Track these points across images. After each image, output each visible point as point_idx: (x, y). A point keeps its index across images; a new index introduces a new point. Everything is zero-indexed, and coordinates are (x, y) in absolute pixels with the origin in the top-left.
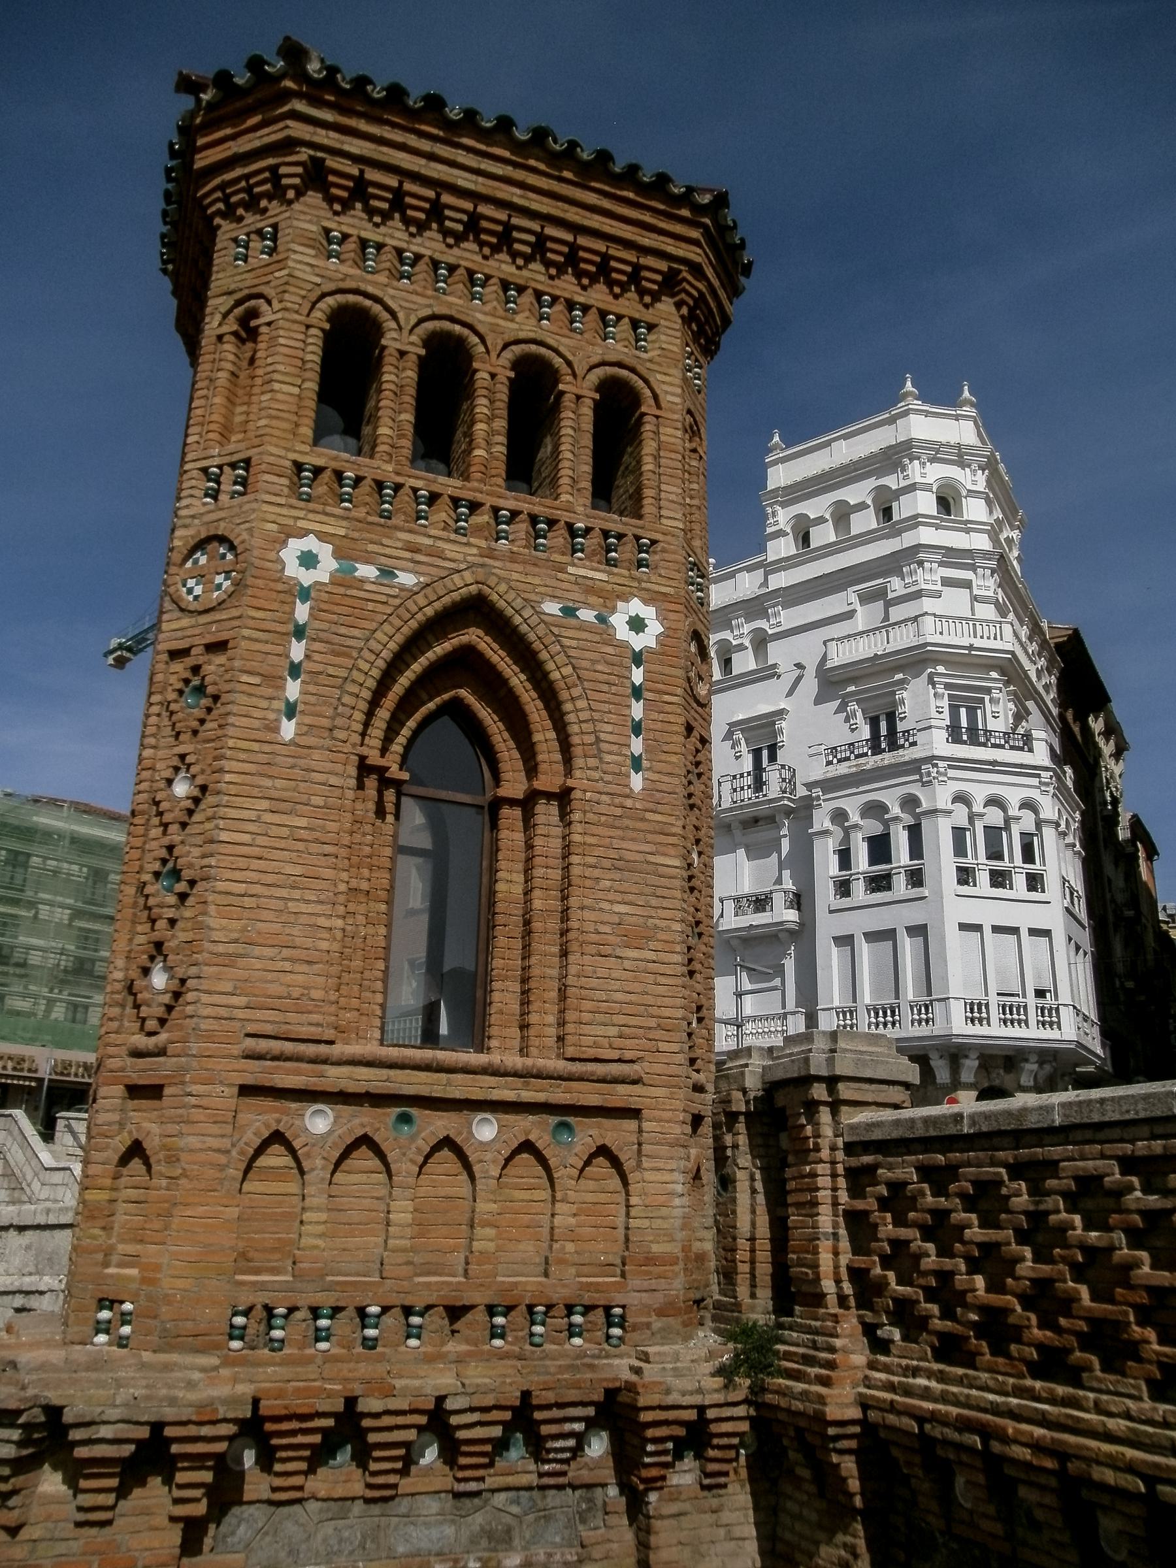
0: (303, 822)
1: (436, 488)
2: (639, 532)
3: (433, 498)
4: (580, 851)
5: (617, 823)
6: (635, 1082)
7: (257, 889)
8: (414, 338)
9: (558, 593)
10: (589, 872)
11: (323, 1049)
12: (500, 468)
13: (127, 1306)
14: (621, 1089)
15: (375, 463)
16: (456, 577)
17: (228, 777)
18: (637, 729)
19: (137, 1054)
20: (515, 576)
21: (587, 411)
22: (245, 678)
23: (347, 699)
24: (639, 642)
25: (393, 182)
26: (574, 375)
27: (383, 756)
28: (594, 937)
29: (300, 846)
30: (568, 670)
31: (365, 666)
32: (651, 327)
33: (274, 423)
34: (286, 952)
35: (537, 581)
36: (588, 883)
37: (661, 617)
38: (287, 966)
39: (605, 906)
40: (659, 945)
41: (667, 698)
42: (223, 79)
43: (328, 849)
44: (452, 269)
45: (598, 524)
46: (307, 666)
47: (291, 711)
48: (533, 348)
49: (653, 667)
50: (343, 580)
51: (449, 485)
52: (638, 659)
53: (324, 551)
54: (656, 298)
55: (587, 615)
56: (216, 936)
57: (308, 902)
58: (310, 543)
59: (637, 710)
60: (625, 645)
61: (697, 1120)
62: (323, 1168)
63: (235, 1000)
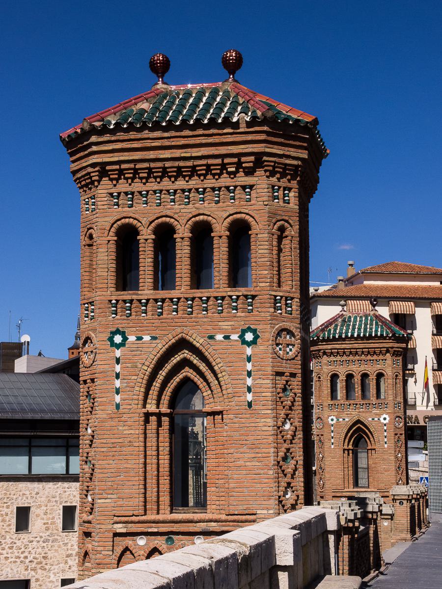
1: (350, 403)
3: (350, 405)
14: (385, 493)
18: (386, 437)
19: (320, 492)
23: (340, 441)
24: (385, 422)
25: (336, 351)
27: (348, 447)
32: (385, 360)
37: (389, 416)
44: (349, 361)
45: (377, 402)
48: (364, 371)
52: (385, 425)
54: (385, 354)
55: (376, 419)
58: (332, 417)
59: (385, 434)
60: (383, 423)
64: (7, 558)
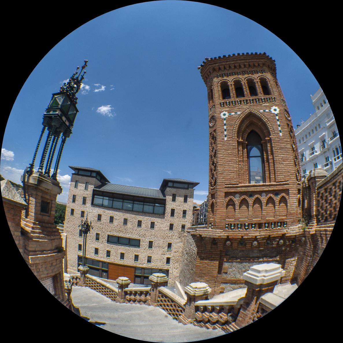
0: (230, 152)
2: (272, 97)
4: (274, 147)
5: (279, 141)
6: (288, 184)
7: (224, 163)
8: (232, 82)
9: (262, 109)
10: (276, 150)
11: (237, 185)
12: (249, 94)
13: (212, 224)
15: (231, 99)
16: (246, 111)
17: (218, 148)
18: (279, 126)
20: (255, 108)
21: (259, 83)
22: (218, 133)
23: (234, 132)
24: (276, 112)
26: (256, 79)
28: (279, 161)
29: (230, 155)
30: (266, 119)
31: (235, 127)
33: (216, 99)
34: (230, 172)
35: (258, 108)
36: (276, 152)
38: (230, 173)
39: (279, 156)
40: (289, 161)
41: (283, 120)
42: (202, 66)
43: (235, 155)
45: (265, 97)
46: (227, 129)
47: (226, 136)
49: (279, 116)
50: (230, 116)
51: (242, 99)
52: (277, 115)
53: (226, 113)
55: (267, 110)
56: (219, 171)
57: (232, 163)
58: (224, 112)
59: (278, 123)
60: (274, 114)
61: (299, 190)
62: (238, 203)
63: (223, 180)
64: (134, 233)
